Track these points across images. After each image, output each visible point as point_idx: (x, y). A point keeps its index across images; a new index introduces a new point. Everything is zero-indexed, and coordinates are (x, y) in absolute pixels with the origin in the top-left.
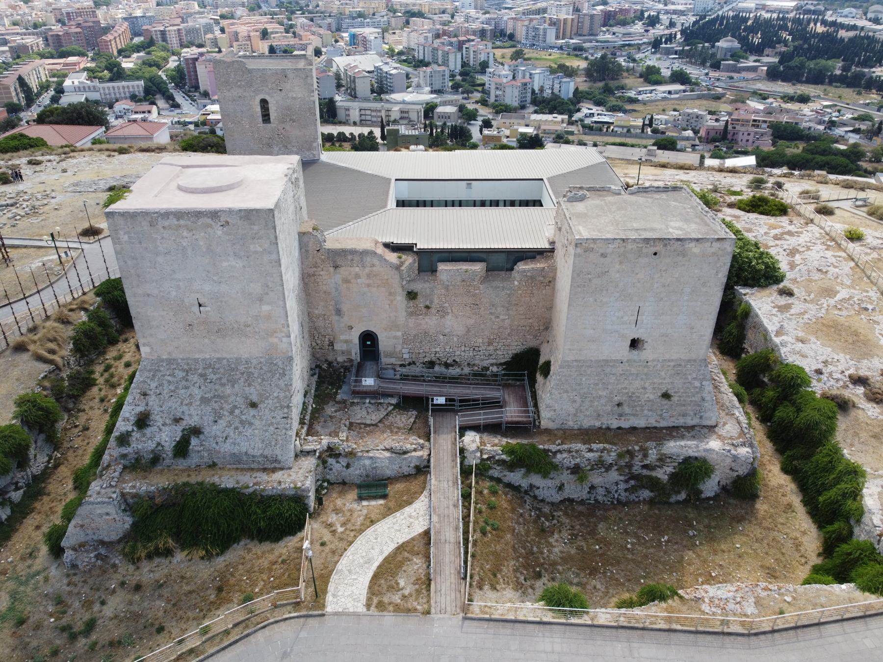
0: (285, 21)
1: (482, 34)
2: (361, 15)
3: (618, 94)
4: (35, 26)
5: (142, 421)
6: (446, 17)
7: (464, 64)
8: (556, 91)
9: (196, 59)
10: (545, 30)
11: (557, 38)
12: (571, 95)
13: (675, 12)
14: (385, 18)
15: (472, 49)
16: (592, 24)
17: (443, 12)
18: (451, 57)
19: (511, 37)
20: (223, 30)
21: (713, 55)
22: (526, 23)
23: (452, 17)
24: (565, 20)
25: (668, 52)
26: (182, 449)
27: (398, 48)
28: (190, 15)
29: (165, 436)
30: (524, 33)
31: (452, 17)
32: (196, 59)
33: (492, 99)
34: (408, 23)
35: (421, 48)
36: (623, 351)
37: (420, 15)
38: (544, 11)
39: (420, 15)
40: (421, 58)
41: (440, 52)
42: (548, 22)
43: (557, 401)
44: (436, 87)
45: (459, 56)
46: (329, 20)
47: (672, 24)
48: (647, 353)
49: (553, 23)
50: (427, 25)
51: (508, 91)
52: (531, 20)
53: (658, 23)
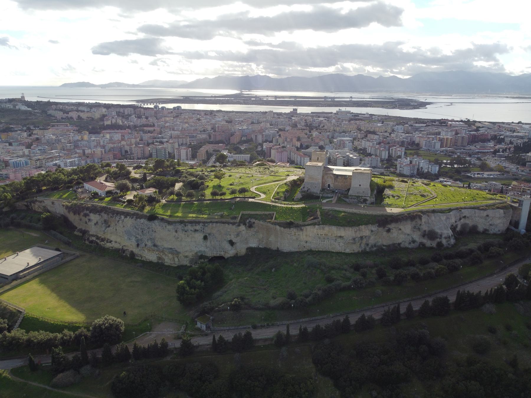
0: (308, 133)
1: (402, 144)
2: (344, 132)
3: (463, 174)
4: (204, 131)
5: (304, 187)
6: (387, 134)
7: (390, 156)
8: (430, 170)
9: (271, 148)
10: (435, 143)
11: (442, 146)
12: (437, 172)
13: (517, 137)
14: (356, 134)
15: (394, 150)
16: (462, 141)
17: (386, 132)
18: (383, 153)
19: (418, 145)
20: (280, 136)
21: (525, 159)
22: (426, 139)
23: (390, 134)
24: (447, 139)
25: (501, 156)
26: (308, 191)
27: (359, 147)
28: (267, 129)
29: (306, 189)
30: (424, 143)
31: (390, 134)
32: (271, 148)
33: (398, 171)
34: (366, 136)
35: (370, 148)
36: (358, 186)
37: (374, 133)
38: (439, 134)
39: (374, 133)
40: (369, 152)
41: (378, 151)
42: (438, 139)
43: (351, 193)
44: (374, 165)
45: (387, 152)
46: (328, 133)
47: (511, 143)
48: (361, 187)
49: (441, 140)
50: (376, 137)
51: (405, 168)
52: (429, 138)
53: (504, 142)
